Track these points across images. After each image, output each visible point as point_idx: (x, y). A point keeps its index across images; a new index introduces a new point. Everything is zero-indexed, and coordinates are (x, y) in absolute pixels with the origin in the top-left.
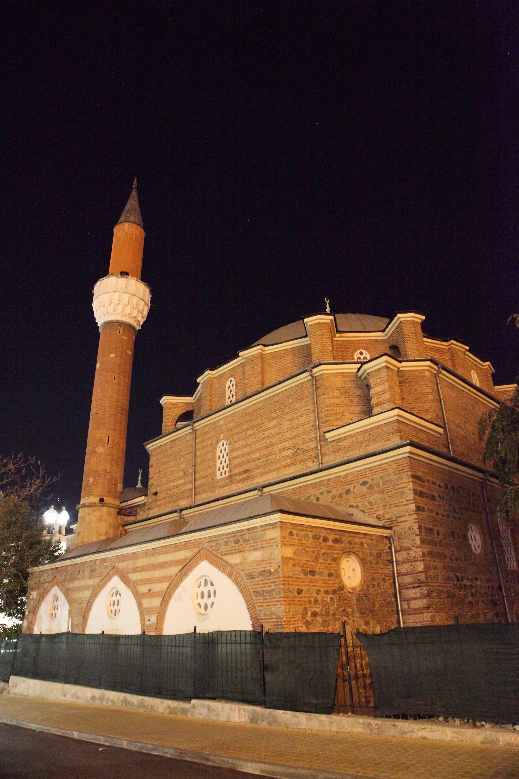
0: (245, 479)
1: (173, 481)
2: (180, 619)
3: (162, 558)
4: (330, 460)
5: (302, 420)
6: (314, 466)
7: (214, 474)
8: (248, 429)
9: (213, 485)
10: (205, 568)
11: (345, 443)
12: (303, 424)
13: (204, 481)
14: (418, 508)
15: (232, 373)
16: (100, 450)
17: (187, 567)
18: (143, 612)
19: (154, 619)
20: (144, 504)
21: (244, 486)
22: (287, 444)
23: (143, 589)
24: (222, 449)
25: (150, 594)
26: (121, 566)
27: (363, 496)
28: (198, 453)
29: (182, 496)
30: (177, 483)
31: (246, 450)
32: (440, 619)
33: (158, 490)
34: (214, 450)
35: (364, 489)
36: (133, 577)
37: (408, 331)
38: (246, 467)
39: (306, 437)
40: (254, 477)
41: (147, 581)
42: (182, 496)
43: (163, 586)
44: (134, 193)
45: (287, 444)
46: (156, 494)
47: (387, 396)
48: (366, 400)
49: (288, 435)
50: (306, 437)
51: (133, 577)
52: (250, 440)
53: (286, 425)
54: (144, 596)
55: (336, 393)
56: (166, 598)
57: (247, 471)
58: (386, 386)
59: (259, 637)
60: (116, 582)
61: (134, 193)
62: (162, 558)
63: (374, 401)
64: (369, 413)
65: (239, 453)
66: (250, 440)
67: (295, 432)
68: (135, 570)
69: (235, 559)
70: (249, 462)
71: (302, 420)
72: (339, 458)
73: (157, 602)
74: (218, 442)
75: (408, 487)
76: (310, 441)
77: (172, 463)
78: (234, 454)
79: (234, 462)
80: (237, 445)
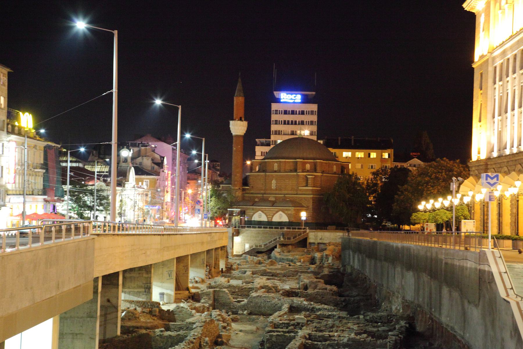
2: (276, 219)
4: (299, 192)
6: (295, 192)
9: (271, 189)
10: (280, 212)
15: (277, 162)
16: (238, 175)
17: (277, 212)
18: (268, 218)
21: (280, 192)
24: (274, 182)
29: (262, 190)
32: (313, 222)
37: (318, 164)
42: (262, 190)
44: (240, 80)
48: (307, 183)
53: (290, 182)
56: (273, 216)
59: (289, 222)
60: (260, 212)
61: (240, 80)
64: (307, 186)
72: (301, 193)
75: (311, 201)
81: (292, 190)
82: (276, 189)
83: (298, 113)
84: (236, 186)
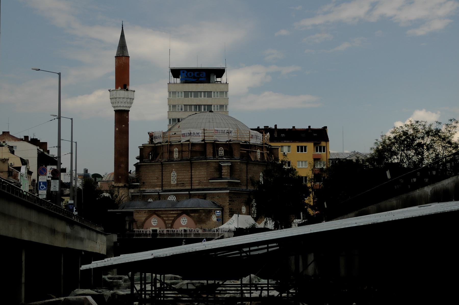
0: (182, 186)
1: (152, 180)
3: (172, 212)
5: (202, 173)
7: (170, 181)
8: (183, 170)
9: (170, 185)
11: (214, 184)
12: (203, 175)
13: (166, 183)
14: (229, 204)
19: (170, 225)
20: (138, 185)
21: (182, 188)
22: (197, 179)
23: (166, 219)
24: (174, 175)
25: (168, 220)
26: (156, 212)
27: (218, 199)
28: (164, 173)
29: (157, 186)
30: (154, 181)
31: (183, 177)
33: (145, 181)
34: (170, 174)
35: (218, 198)
36: (162, 216)
38: (183, 182)
39: (203, 179)
40: (186, 186)
41: (167, 217)
43: (173, 218)
45: (197, 179)
46: (144, 183)
47: (226, 174)
49: (198, 176)
50: (203, 179)
51: (162, 216)
52: (185, 174)
54: (166, 220)
55: (213, 168)
57: (183, 184)
58: (226, 171)
62: (172, 212)
63: (223, 174)
65: (180, 177)
66: (185, 174)
67: (200, 176)
68: (162, 214)
69: (193, 215)
70: (184, 181)
71: (202, 173)
73: (171, 222)
74: (172, 171)
76: (204, 180)
77: (151, 173)
78: (178, 177)
79: (178, 180)
80: (180, 174)
81: (200, 183)
82: (177, 185)
83: (203, 93)
84: (120, 182)
